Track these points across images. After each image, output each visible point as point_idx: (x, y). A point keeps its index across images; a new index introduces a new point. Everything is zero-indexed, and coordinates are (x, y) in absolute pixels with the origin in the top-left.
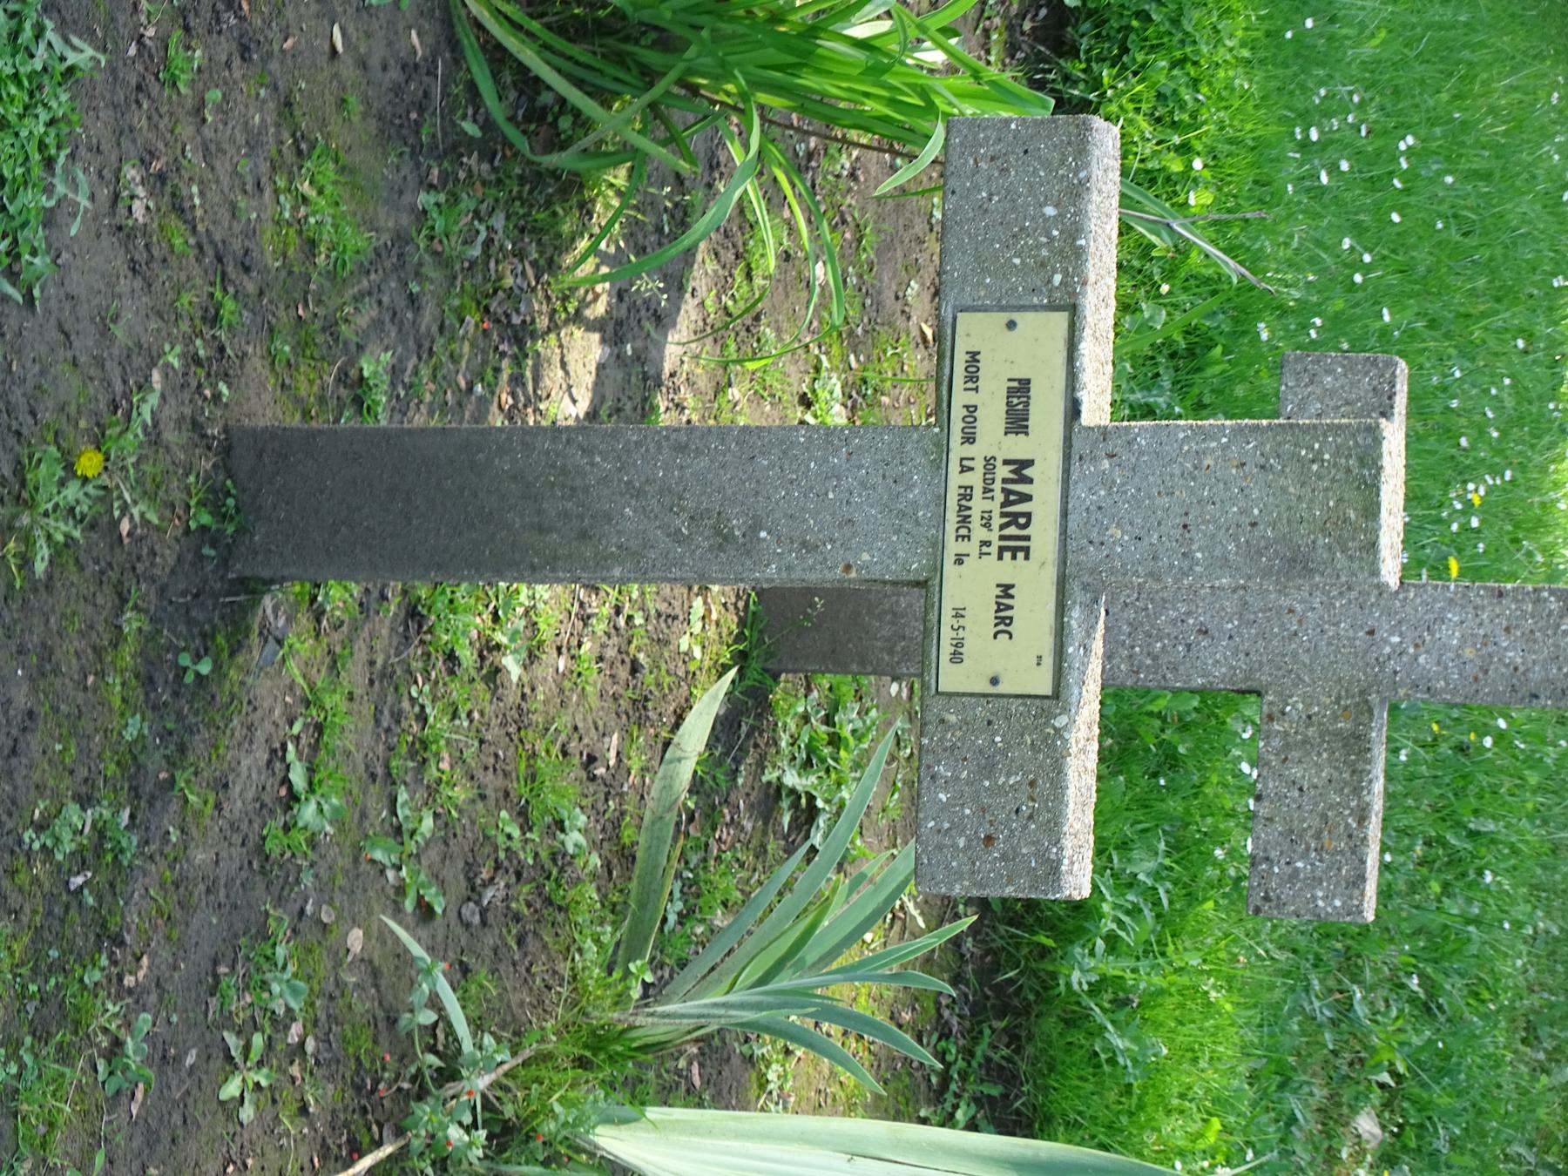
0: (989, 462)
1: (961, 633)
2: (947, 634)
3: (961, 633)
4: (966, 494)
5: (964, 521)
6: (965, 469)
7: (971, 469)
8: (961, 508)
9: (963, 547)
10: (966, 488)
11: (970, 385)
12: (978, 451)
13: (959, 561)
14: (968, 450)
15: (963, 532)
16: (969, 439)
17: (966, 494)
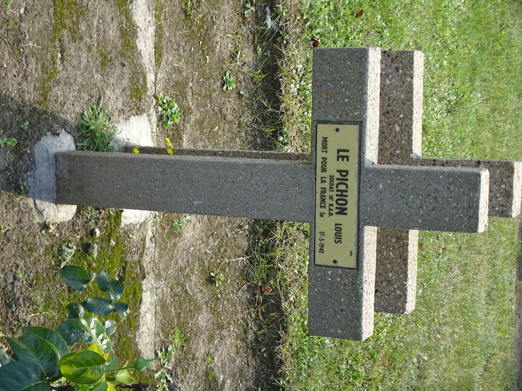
0: (332, 177)
1: (323, 242)
2: (318, 242)
3: (323, 242)
4: (324, 191)
5: (323, 201)
6: (323, 182)
7: (326, 182)
8: (322, 196)
9: (323, 210)
10: (323, 188)
11: (324, 150)
12: (327, 175)
13: (322, 215)
14: (324, 174)
15: (323, 205)
16: (324, 170)
17: (324, 191)
